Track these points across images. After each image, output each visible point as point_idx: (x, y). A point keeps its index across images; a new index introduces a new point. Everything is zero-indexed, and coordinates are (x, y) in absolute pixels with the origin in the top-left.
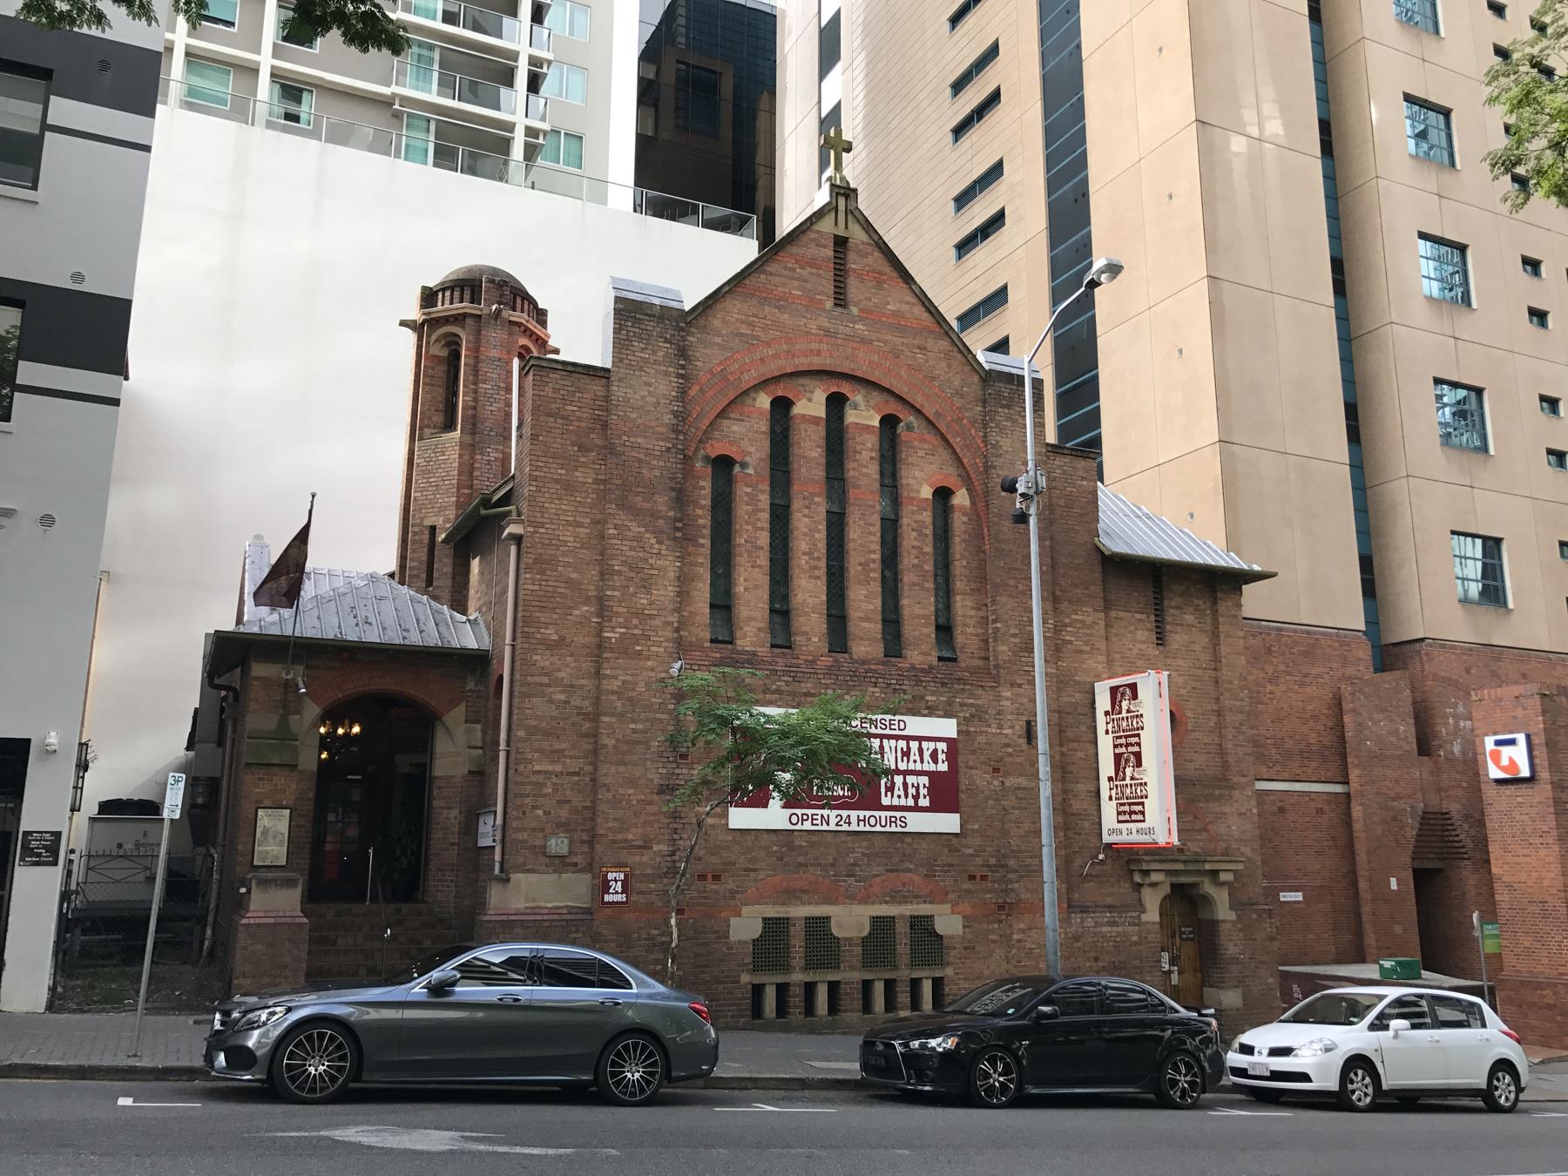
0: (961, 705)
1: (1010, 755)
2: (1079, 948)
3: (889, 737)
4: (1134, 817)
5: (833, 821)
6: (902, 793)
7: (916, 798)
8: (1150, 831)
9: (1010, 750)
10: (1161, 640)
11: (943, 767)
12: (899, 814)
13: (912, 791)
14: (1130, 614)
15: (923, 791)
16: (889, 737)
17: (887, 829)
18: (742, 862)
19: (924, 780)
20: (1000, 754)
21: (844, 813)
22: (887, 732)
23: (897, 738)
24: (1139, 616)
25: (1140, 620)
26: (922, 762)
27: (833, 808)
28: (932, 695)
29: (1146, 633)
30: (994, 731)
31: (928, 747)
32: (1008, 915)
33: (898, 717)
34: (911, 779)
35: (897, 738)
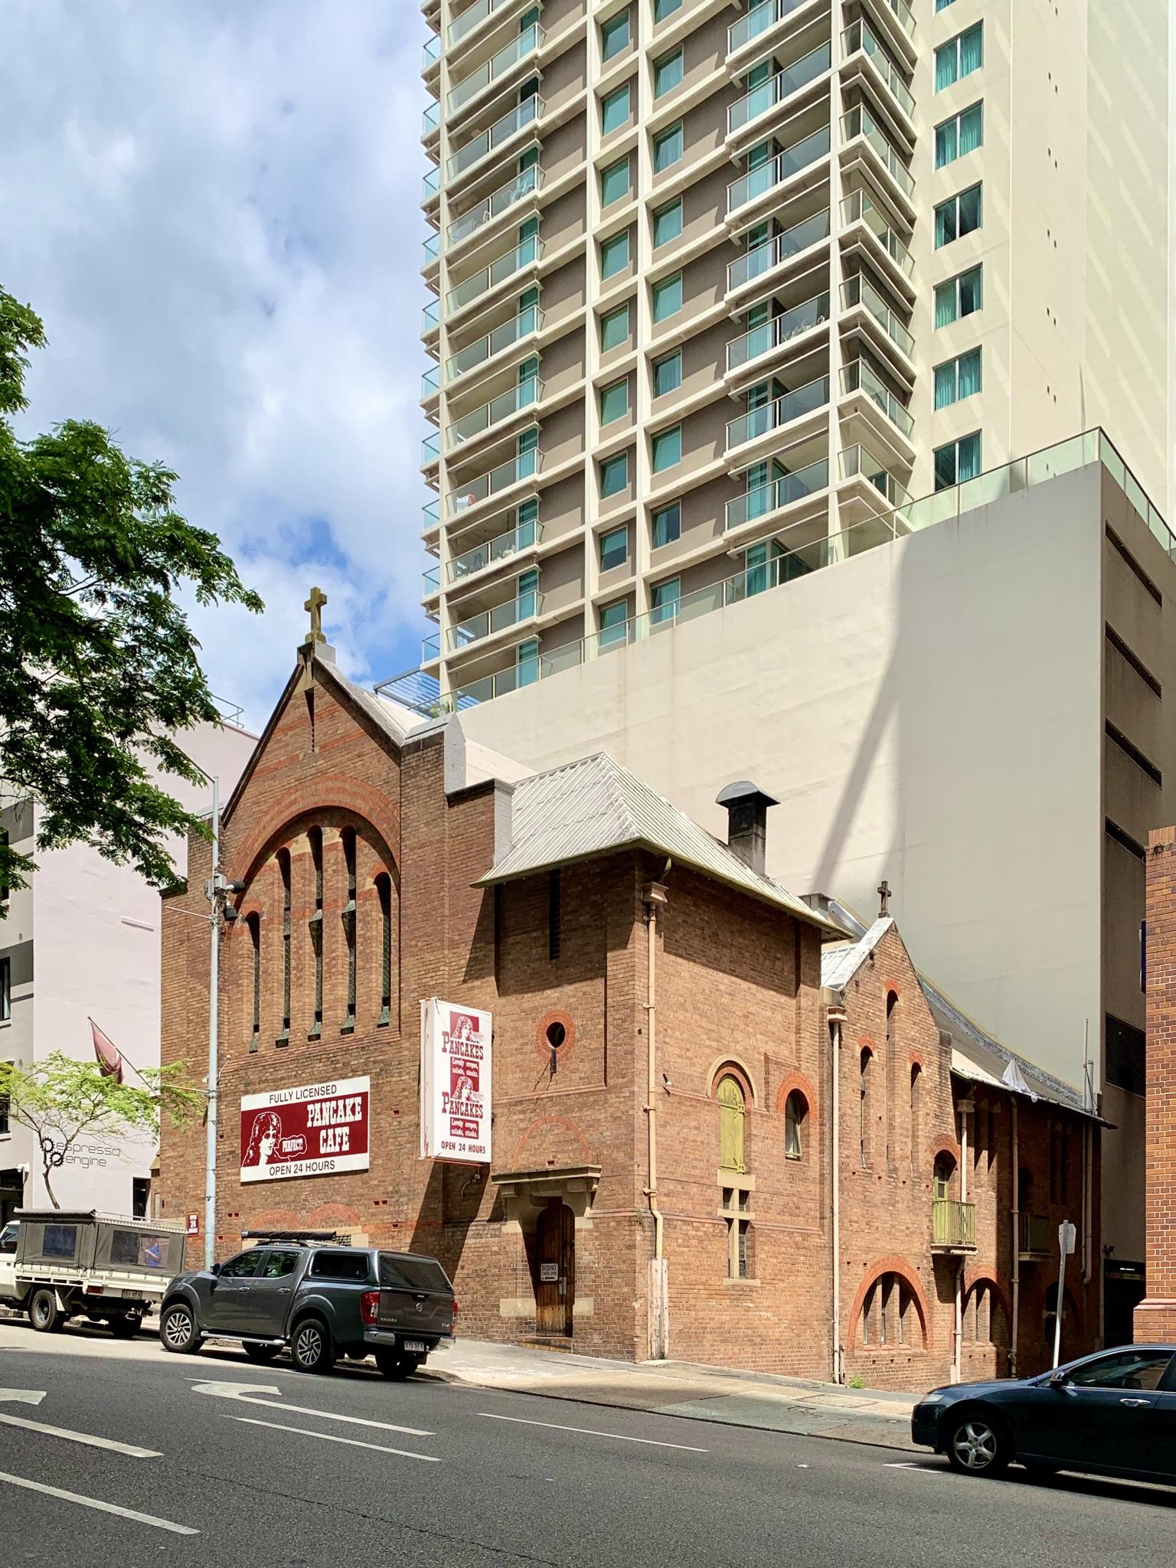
0: (374, 1062)
1: (406, 1097)
2: (450, 1258)
3: (326, 1100)
4: (467, 1133)
5: (293, 1169)
6: (332, 1143)
7: (341, 1145)
8: (481, 1150)
9: (406, 1093)
10: (554, 953)
11: (358, 1117)
12: (329, 1159)
13: (338, 1140)
14: (525, 936)
15: (346, 1139)
16: (326, 1100)
17: (323, 1172)
18: (248, 1204)
19: (346, 1130)
20: (399, 1098)
21: (299, 1163)
22: (326, 1096)
23: (330, 1100)
24: (534, 934)
25: (535, 938)
26: (345, 1115)
27: (293, 1160)
28: (355, 1060)
29: (540, 950)
30: (395, 1079)
31: (349, 1102)
32: (399, 1232)
33: (330, 1084)
34: (338, 1131)
35: (330, 1100)
